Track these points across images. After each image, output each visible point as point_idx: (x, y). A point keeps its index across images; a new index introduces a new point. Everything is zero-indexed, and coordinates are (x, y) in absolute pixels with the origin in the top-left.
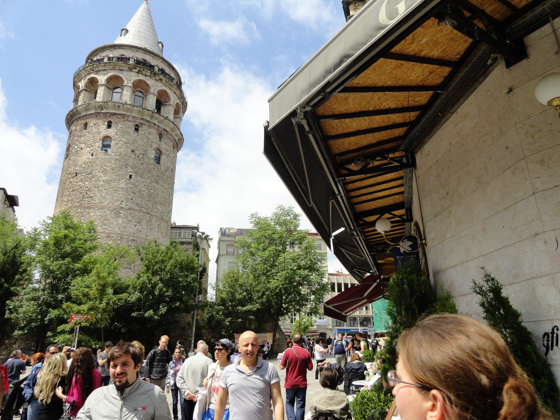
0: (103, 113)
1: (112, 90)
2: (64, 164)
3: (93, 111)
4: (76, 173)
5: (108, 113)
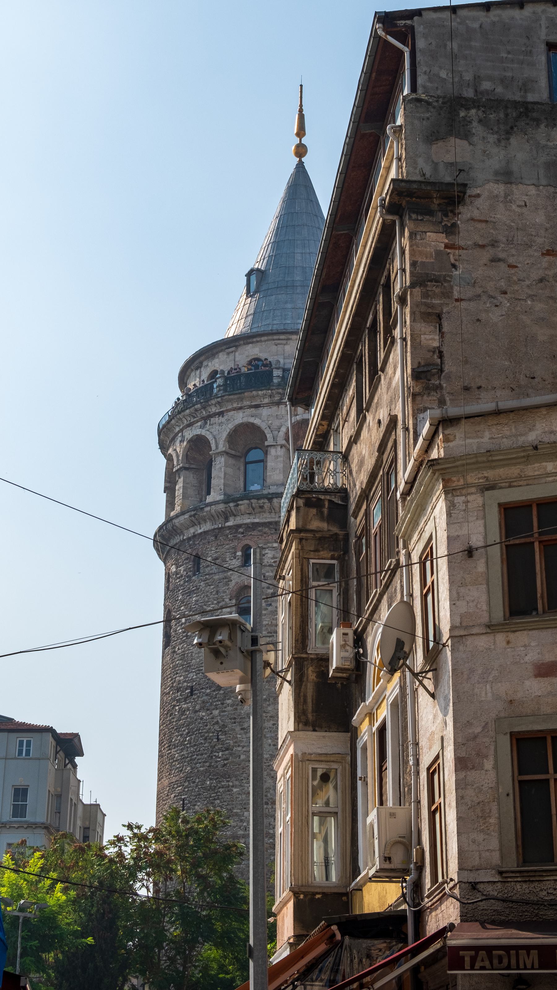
0: (230, 528)
1: (242, 460)
2: (164, 662)
3: (207, 527)
4: (192, 688)
5: (239, 526)
